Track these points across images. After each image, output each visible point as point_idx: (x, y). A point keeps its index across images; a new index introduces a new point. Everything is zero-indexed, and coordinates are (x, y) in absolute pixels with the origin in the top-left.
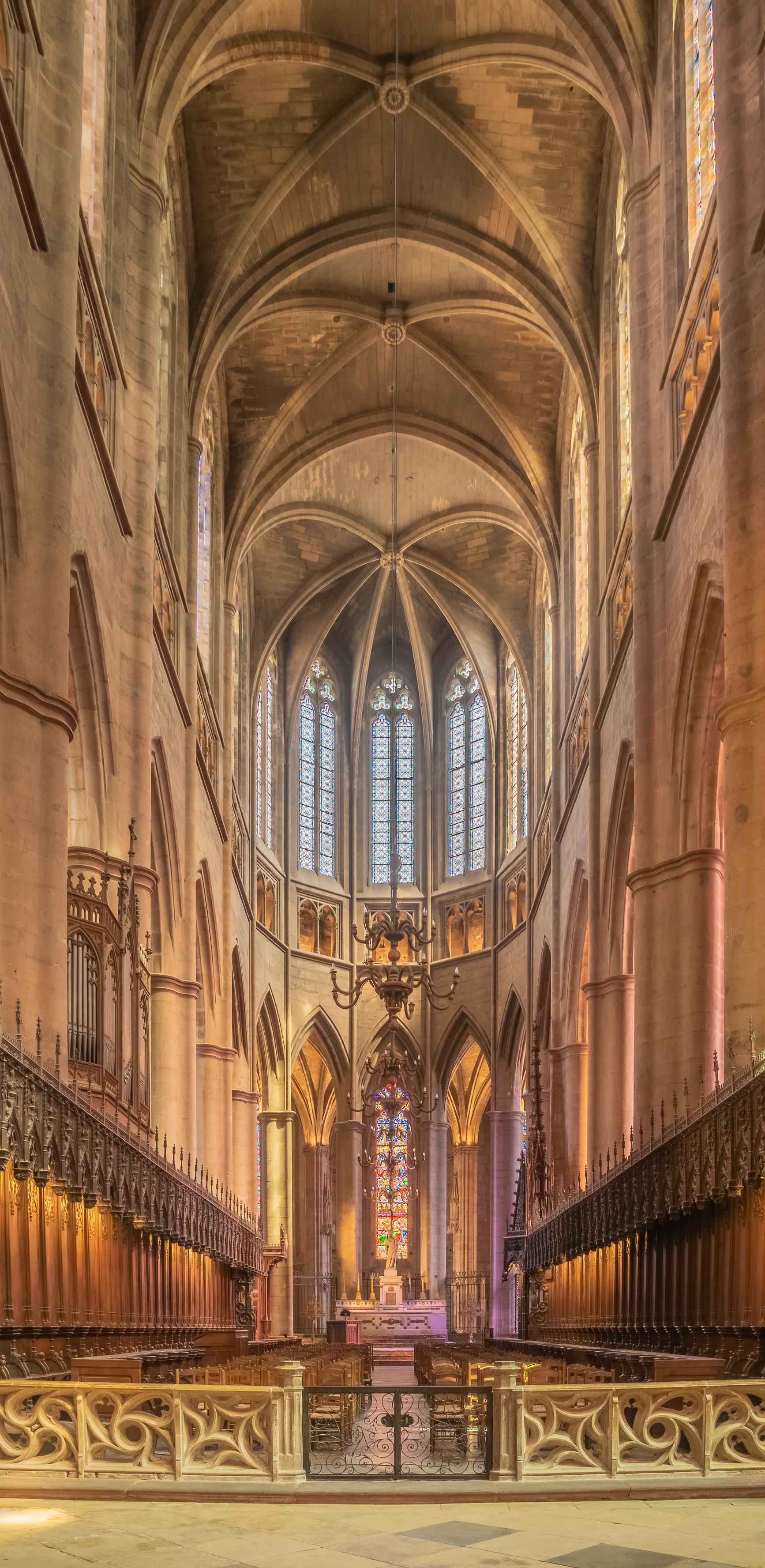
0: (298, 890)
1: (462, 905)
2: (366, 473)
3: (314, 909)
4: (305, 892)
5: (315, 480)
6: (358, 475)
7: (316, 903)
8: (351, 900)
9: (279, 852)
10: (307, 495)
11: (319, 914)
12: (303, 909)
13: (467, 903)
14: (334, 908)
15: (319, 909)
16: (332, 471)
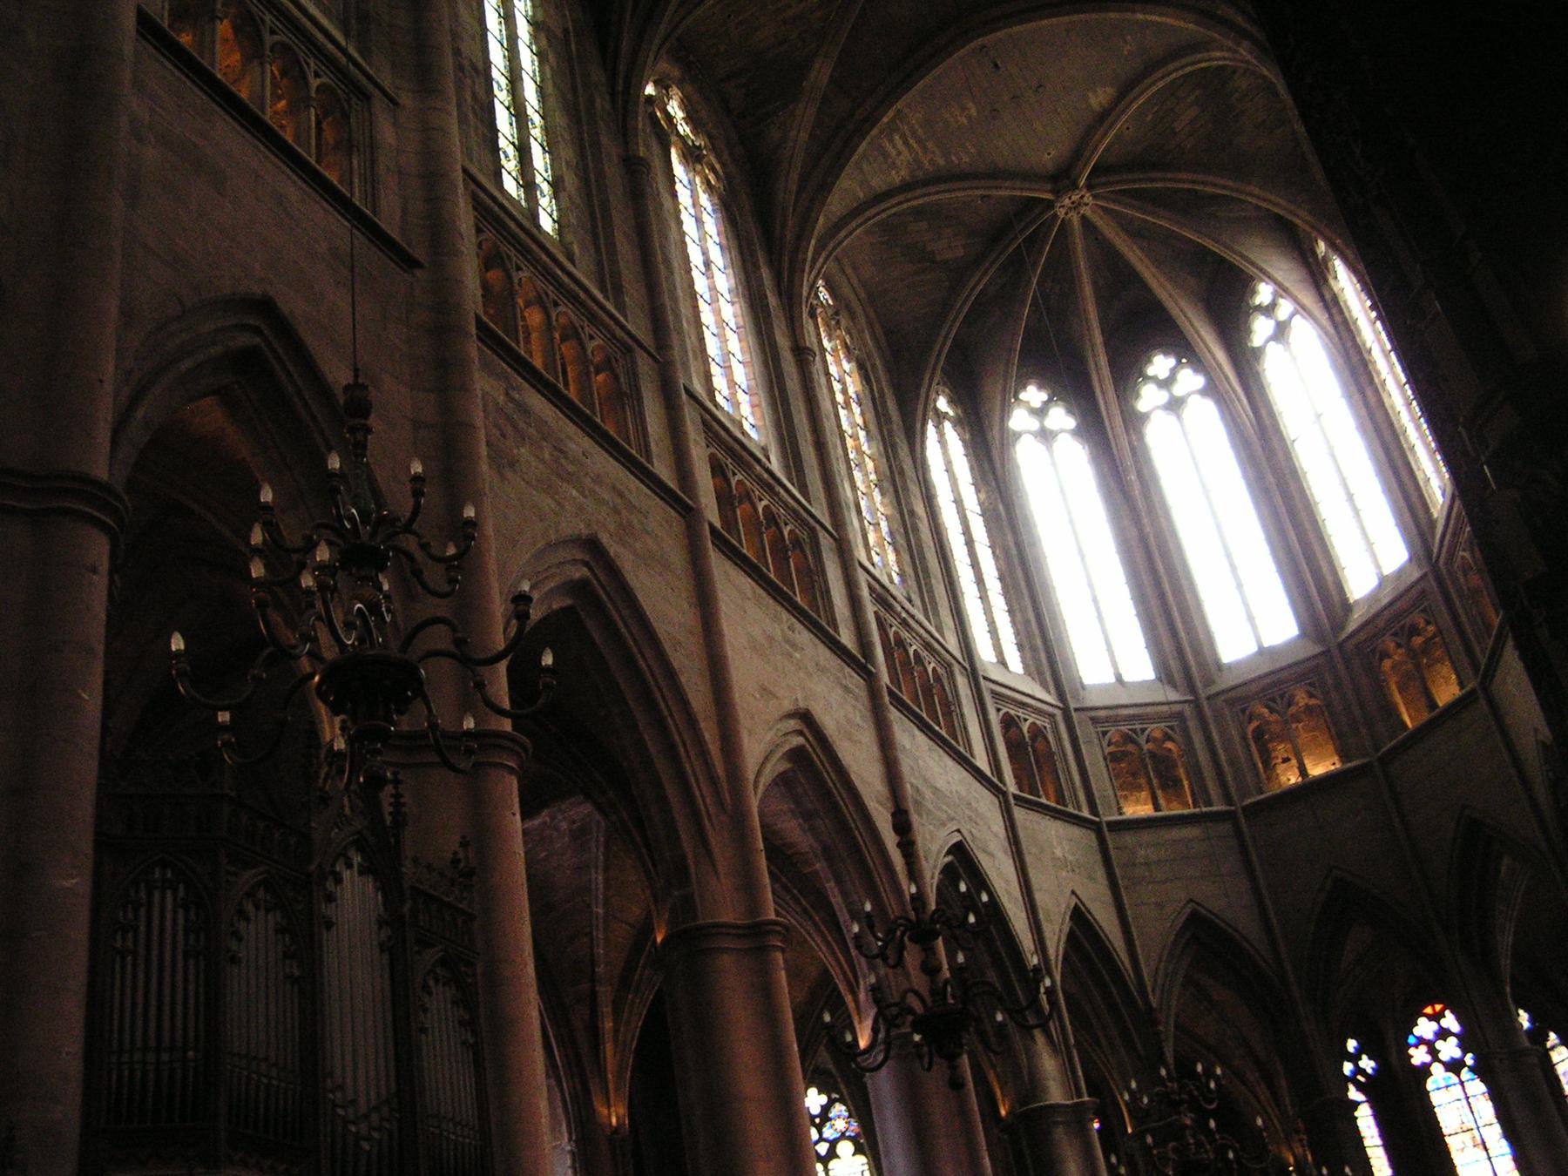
0: (1094, 720)
1: (1395, 634)
2: (973, 112)
3: (1133, 741)
4: (1107, 719)
5: (899, 154)
6: (965, 120)
7: (1134, 731)
8: (1196, 703)
9: (1040, 674)
10: (896, 178)
11: (1146, 747)
12: (1112, 748)
13: (1402, 628)
14: (1171, 728)
15: (1142, 740)
16: (920, 132)
